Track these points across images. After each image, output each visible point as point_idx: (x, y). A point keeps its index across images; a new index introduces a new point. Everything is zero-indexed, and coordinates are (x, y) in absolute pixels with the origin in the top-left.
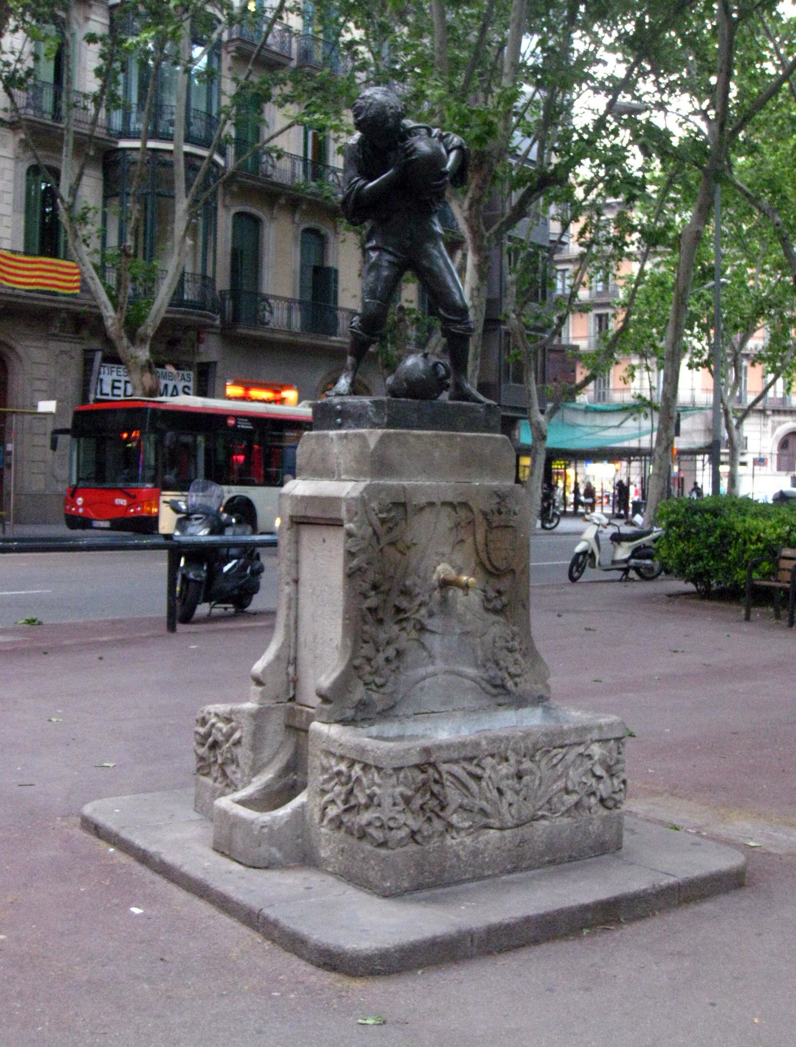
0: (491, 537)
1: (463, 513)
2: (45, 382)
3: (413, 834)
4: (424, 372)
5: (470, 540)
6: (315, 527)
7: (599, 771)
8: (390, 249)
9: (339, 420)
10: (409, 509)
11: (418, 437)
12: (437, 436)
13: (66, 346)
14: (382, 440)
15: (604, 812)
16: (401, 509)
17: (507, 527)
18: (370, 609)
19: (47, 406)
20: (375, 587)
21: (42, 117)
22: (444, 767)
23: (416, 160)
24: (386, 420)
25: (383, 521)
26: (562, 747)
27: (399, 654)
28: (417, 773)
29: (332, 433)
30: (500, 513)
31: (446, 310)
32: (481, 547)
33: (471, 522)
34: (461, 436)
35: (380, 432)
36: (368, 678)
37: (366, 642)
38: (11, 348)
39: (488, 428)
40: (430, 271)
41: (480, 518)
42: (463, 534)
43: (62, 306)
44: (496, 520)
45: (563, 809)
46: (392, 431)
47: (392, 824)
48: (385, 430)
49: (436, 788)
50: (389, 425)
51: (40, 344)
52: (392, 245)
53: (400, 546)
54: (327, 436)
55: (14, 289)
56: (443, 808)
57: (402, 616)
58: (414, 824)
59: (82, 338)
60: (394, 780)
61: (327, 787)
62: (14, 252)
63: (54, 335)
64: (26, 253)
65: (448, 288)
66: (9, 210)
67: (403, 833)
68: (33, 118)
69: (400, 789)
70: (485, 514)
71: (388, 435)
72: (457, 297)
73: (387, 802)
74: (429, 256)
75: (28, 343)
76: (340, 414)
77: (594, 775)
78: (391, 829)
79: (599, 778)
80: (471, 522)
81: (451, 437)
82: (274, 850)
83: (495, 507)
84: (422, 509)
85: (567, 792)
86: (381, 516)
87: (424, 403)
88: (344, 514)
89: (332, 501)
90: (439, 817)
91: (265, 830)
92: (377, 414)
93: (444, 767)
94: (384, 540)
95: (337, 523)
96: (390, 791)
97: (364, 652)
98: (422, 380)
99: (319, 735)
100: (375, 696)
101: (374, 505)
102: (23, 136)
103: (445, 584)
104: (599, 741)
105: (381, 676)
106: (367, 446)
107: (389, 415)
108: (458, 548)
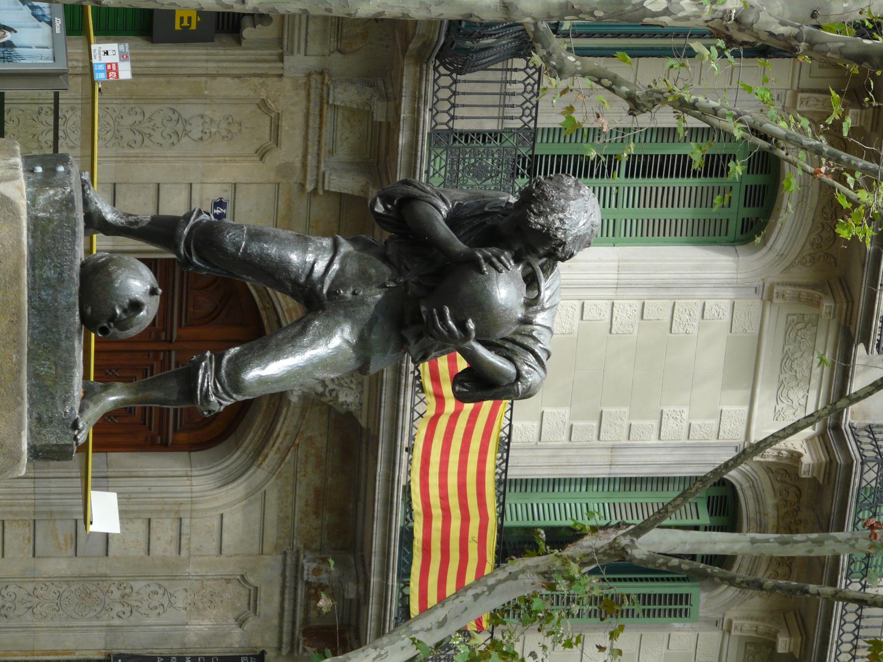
2: (172, 550)
8: (336, 267)
9: (39, 169)
11: (17, 278)
12: (18, 314)
13: (270, 605)
19: (105, 513)
21: (859, 509)
23: (483, 273)
24: (41, 214)
31: (236, 357)
34: (19, 363)
35: (23, 204)
38: (258, 453)
39: (39, 422)
40: (303, 332)
43: (374, 580)
46: (25, 224)
51: (271, 533)
52: (342, 270)
55: (410, 450)
59: (293, 645)
62: (505, 445)
63: (298, 568)
64: (504, 484)
65: (276, 358)
66: (614, 434)
68: (855, 480)
71: (16, 214)
74: (328, 333)
75: (272, 498)
81: (16, 342)
87: (75, 289)
92: (51, 203)
98: (112, 282)
102: (807, 459)
107: (50, 220)
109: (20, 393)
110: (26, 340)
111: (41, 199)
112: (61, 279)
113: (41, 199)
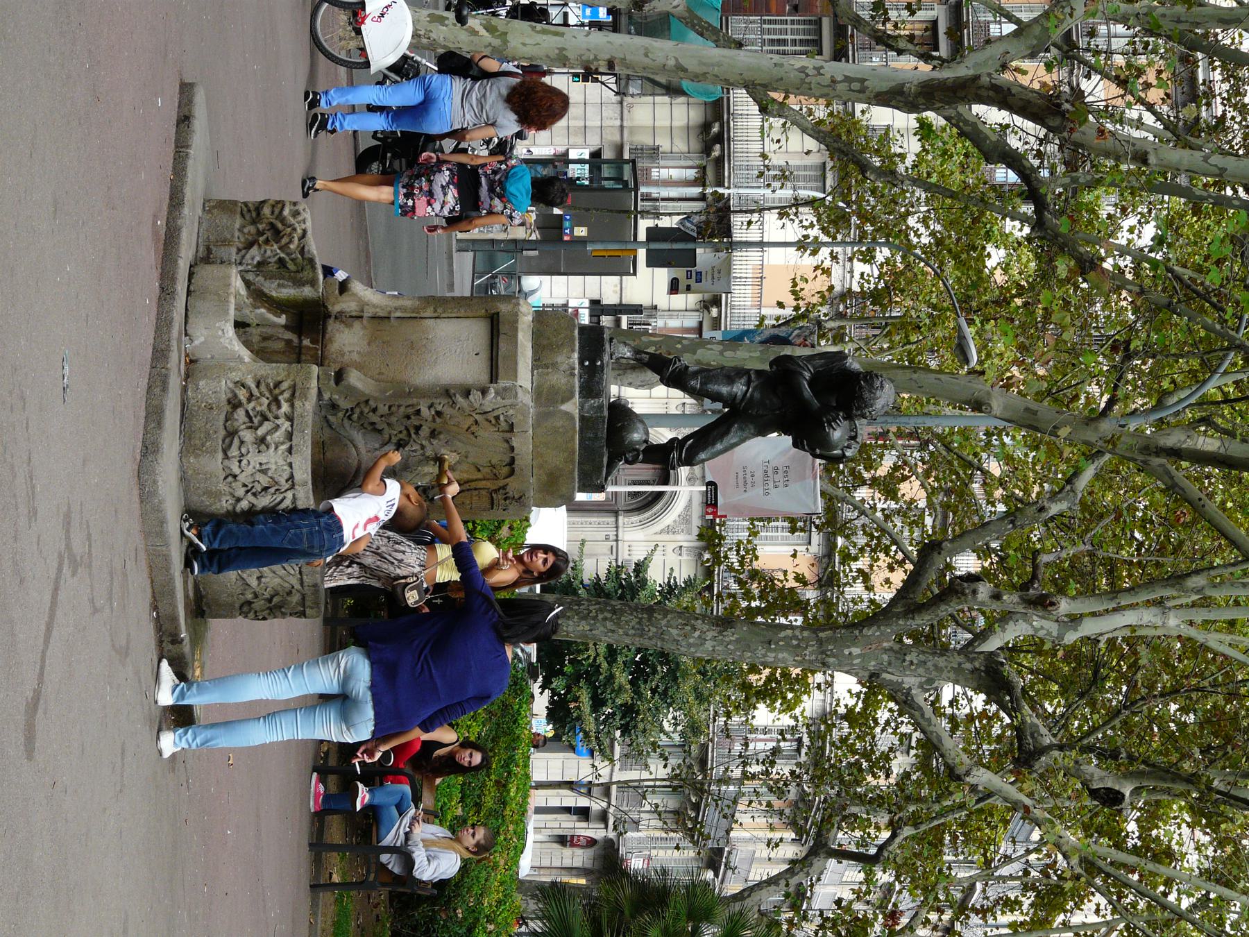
0: (484, 492)
1: (506, 470)
3: (235, 476)
4: (632, 442)
5: (480, 476)
6: (488, 342)
7: (275, 600)
10: (508, 435)
11: (573, 439)
14: (569, 416)
15: (237, 606)
16: (507, 428)
17: (492, 504)
18: (419, 411)
20: (439, 414)
22: (289, 495)
25: (497, 418)
26: (300, 573)
27: (380, 431)
28: (286, 476)
29: (576, 355)
30: (505, 499)
32: (473, 485)
33: (496, 477)
36: (357, 411)
37: (390, 407)
41: (501, 483)
42: (486, 470)
44: (498, 497)
45: (245, 576)
47: (244, 462)
48: (577, 417)
49: (272, 490)
50: (582, 418)
53: (474, 428)
54: (573, 351)
56: (254, 495)
57: (412, 432)
58: (242, 478)
60: (281, 462)
61: (263, 388)
67: (236, 470)
69: (273, 467)
70: (504, 487)
71: (573, 418)
72: (703, 456)
73: (263, 458)
76: (593, 362)
77: (272, 597)
78: (240, 461)
79: (270, 600)
80: (496, 477)
81: (573, 461)
82: (202, 339)
83: (511, 494)
84: (508, 442)
85: (259, 578)
86: (502, 418)
88: (503, 383)
89: (514, 374)
90: (247, 492)
91: (220, 333)
92: (592, 407)
93: (289, 495)
94: (477, 417)
95: (494, 377)
96: (273, 461)
97: (380, 406)
99: (308, 378)
100: (341, 414)
101: (511, 412)
103: (439, 460)
104: (303, 599)
105: (359, 418)
106: (563, 402)
108: (473, 469)
109: (574, 478)
110: (577, 458)
111: (587, 406)
112: (596, 438)
113: (587, 406)
